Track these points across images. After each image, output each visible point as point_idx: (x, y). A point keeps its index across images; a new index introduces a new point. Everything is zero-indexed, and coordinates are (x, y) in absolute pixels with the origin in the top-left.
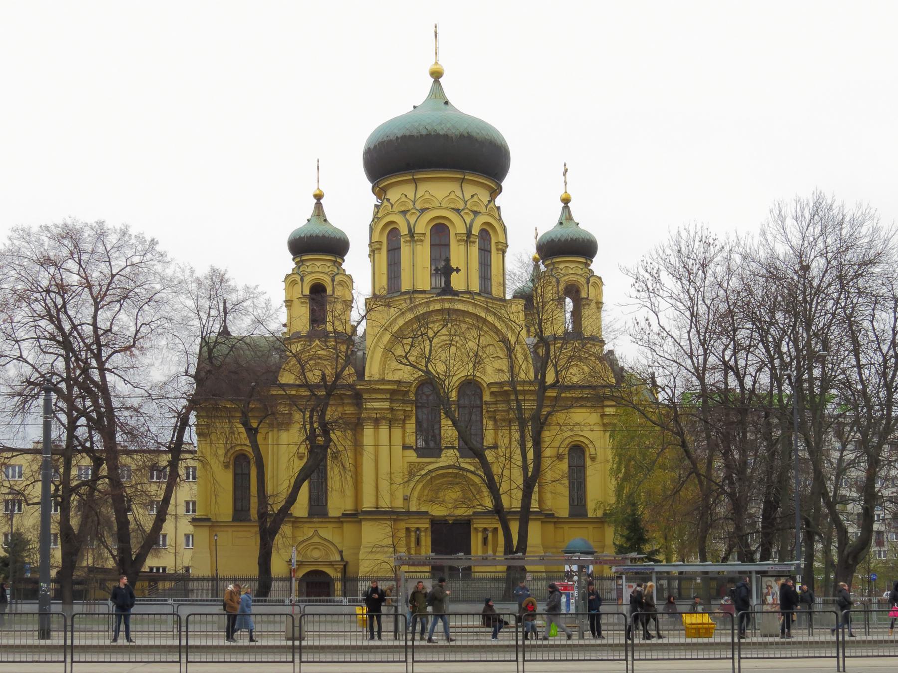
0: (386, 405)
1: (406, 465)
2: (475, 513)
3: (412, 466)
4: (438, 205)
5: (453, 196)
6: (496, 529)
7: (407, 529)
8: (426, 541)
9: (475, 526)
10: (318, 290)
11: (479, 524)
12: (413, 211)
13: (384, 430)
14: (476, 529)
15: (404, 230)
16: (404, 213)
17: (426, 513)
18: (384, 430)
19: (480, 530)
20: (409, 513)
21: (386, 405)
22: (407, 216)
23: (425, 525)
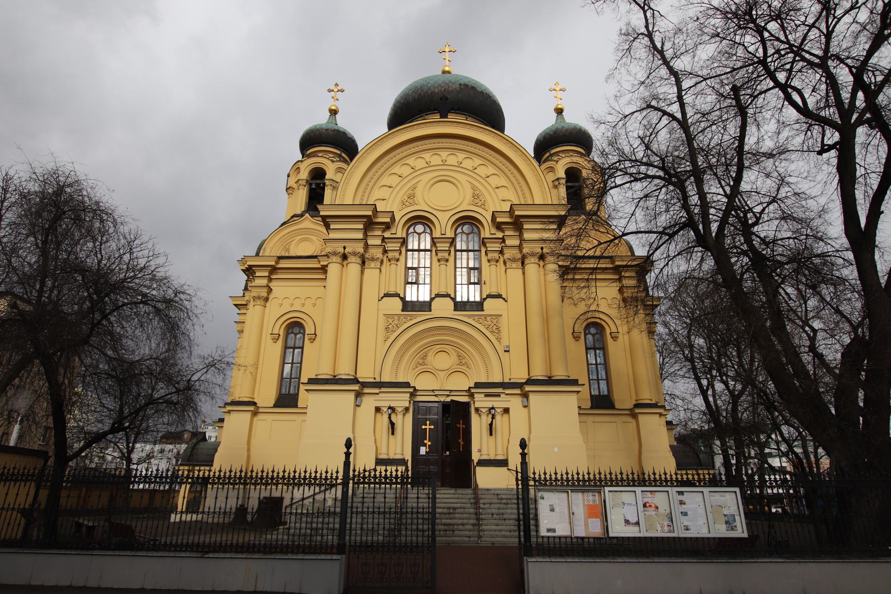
1: (382, 319)
2: (478, 385)
3: (390, 321)
6: (506, 411)
7: (378, 410)
8: (405, 425)
9: (477, 405)
10: (318, 174)
11: (481, 401)
13: (354, 267)
14: (477, 410)
17: (407, 385)
18: (354, 267)
19: (484, 410)
20: (380, 385)
23: (401, 400)
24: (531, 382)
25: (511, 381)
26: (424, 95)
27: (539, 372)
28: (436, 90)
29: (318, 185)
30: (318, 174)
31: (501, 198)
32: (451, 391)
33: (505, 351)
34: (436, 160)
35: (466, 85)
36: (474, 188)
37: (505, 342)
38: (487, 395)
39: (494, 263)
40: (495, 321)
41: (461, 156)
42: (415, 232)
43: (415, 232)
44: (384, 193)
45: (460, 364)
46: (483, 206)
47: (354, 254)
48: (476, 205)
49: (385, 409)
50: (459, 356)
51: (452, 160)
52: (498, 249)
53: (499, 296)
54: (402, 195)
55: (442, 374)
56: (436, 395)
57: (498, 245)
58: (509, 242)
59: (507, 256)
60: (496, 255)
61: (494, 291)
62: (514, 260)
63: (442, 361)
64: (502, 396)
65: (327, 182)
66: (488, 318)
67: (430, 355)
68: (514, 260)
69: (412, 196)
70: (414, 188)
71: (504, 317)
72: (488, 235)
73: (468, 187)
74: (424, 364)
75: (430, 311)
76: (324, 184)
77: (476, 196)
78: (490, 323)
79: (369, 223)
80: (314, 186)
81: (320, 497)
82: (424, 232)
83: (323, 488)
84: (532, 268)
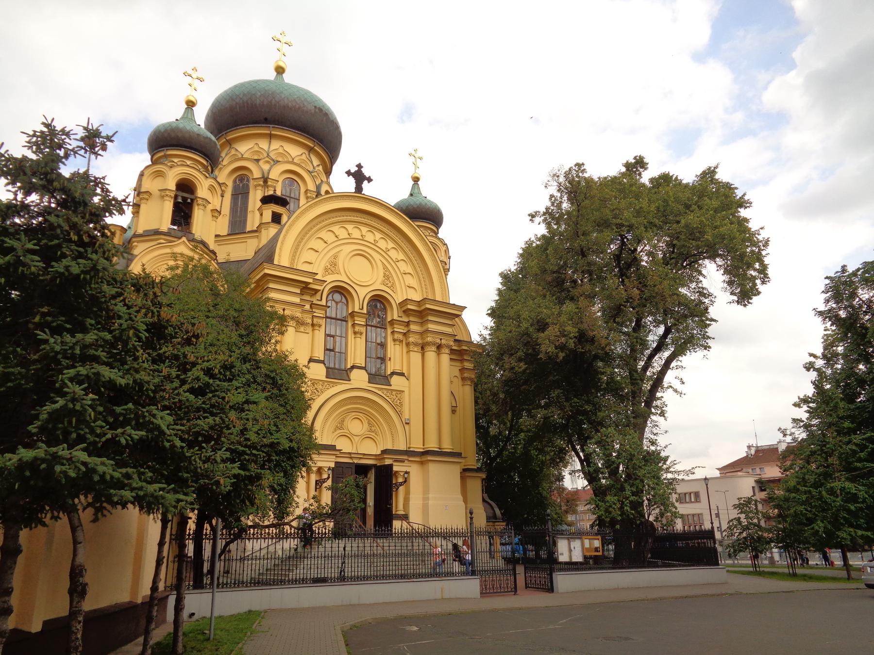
0: (297, 300)
2: (384, 452)
4: (290, 160)
5: (304, 157)
12: (267, 159)
15: (257, 174)
16: (258, 161)
17: (332, 448)
21: (297, 300)
22: (261, 163)
24: (427, 453)
25: (411, 449)
26: (275, 105)
27: (432, 445)
28: (290, 104)
29: (184, 199)
30: (185, 187)
31: (407, 284)
32: (364, 454)
33: (406, 423)
34: (356, 234)
35: (321, 110)
36: (385, 267)
37: (406, 415)
38: (396, 461)
39: (398, 343)
40: (399, 396)
41: (378, 236)
42: (333, 300)
43: (333, 300)
44: (307, 256)
45: (371, 431)
46: (392, 287)
47: (293, 318)
48: (386, 285)
49: (326, 469)
50: (369, 424)
51: (370, 237)
52: (402, 331)
53: (402, 374)
54: (325, 262)
55: (357, 439)
56: (351, 458)
57: (403, 327)
58: (413, 327)
59: (411, 340)
60: (401, 337)
61: (398, 369)
62: (416, 344)
63: (356, 427)
64: (406, 462)
65: (200, 201)
66: (394, 393)
67: (346, 420)
68: (416, 344)
69: (334, 264)
70: (335, 257)
71: (406, 393)
72: (396, 317)
73: (380, 264)
74: (341, 428)
75: (350, 380)
76: (192, 200)
77: (387, 277)
78: (395, 397)
79: (305, 288)
80: (180, 200)
81: (271, 549)
82: (341, 302)
83: (274, 541)
84: (431, 355)
